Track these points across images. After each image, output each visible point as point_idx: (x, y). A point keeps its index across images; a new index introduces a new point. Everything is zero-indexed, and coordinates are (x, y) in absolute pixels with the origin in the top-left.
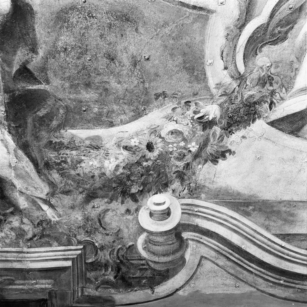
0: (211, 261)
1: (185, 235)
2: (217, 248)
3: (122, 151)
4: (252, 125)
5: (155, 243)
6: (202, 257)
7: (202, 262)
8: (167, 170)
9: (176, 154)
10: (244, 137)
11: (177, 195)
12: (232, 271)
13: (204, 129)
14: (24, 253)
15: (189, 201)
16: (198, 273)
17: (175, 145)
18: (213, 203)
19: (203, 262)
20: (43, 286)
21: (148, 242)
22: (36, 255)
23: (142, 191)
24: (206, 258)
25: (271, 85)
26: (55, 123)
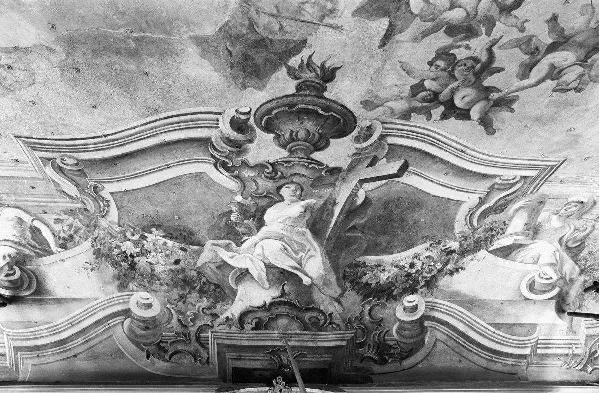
1: (426, 323)
2: (447, 333)
4: (478, 252)
5: (405, 329)
6: (437, 339)
7: (437, 343)
9: (427, 270)
10: (472, 260)
11: (424, 295)
12: (457, 350)
13: (447, 255)
14: (316, 335)
16: (433, 351)
20: (326, 359)
22: (324, 336)
24: (439, 340)
25: (492, 232)
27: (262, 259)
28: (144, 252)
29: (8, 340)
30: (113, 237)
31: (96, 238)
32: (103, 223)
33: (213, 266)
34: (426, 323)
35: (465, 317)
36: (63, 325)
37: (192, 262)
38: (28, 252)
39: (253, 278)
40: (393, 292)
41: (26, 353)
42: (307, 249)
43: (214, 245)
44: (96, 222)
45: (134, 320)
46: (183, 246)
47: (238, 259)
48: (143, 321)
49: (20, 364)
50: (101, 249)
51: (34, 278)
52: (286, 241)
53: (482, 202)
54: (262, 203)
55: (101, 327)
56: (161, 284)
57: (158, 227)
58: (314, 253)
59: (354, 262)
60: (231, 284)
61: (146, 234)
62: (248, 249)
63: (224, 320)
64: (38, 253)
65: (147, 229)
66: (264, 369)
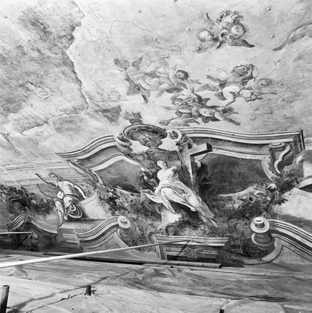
0: (287, 247)
1: (273, 235)
2: (289, 242)
3: (240, 201)
5: (260, 238)
6: (282, 245)
7: (283, 248)
8: (260, 207)
10: (290, 194)
11: (266, 217)
12: (299, 254)
13: (271, 192)
14: (206, 239)
15: (272, 220)
16: (282, 253)
17: (261, 198)
18: (283, 221)
19: (283, 248)
20: (214, 253)
21: (256, 237)
22: (211, 240)
23: (250, 216)
24: (284, 246)
25: (294, 176)
26: (215, 193)
32: (98, 184)
33: (147, 203)
34: (273, 235)
35: (299, 232)
39: (166, 208)
46: (131, 193)
54: (154, 170)
57: (118, 185)
58: (190, 194)
61: (116, 189)
62: (158, 193)
65: (115, 187)
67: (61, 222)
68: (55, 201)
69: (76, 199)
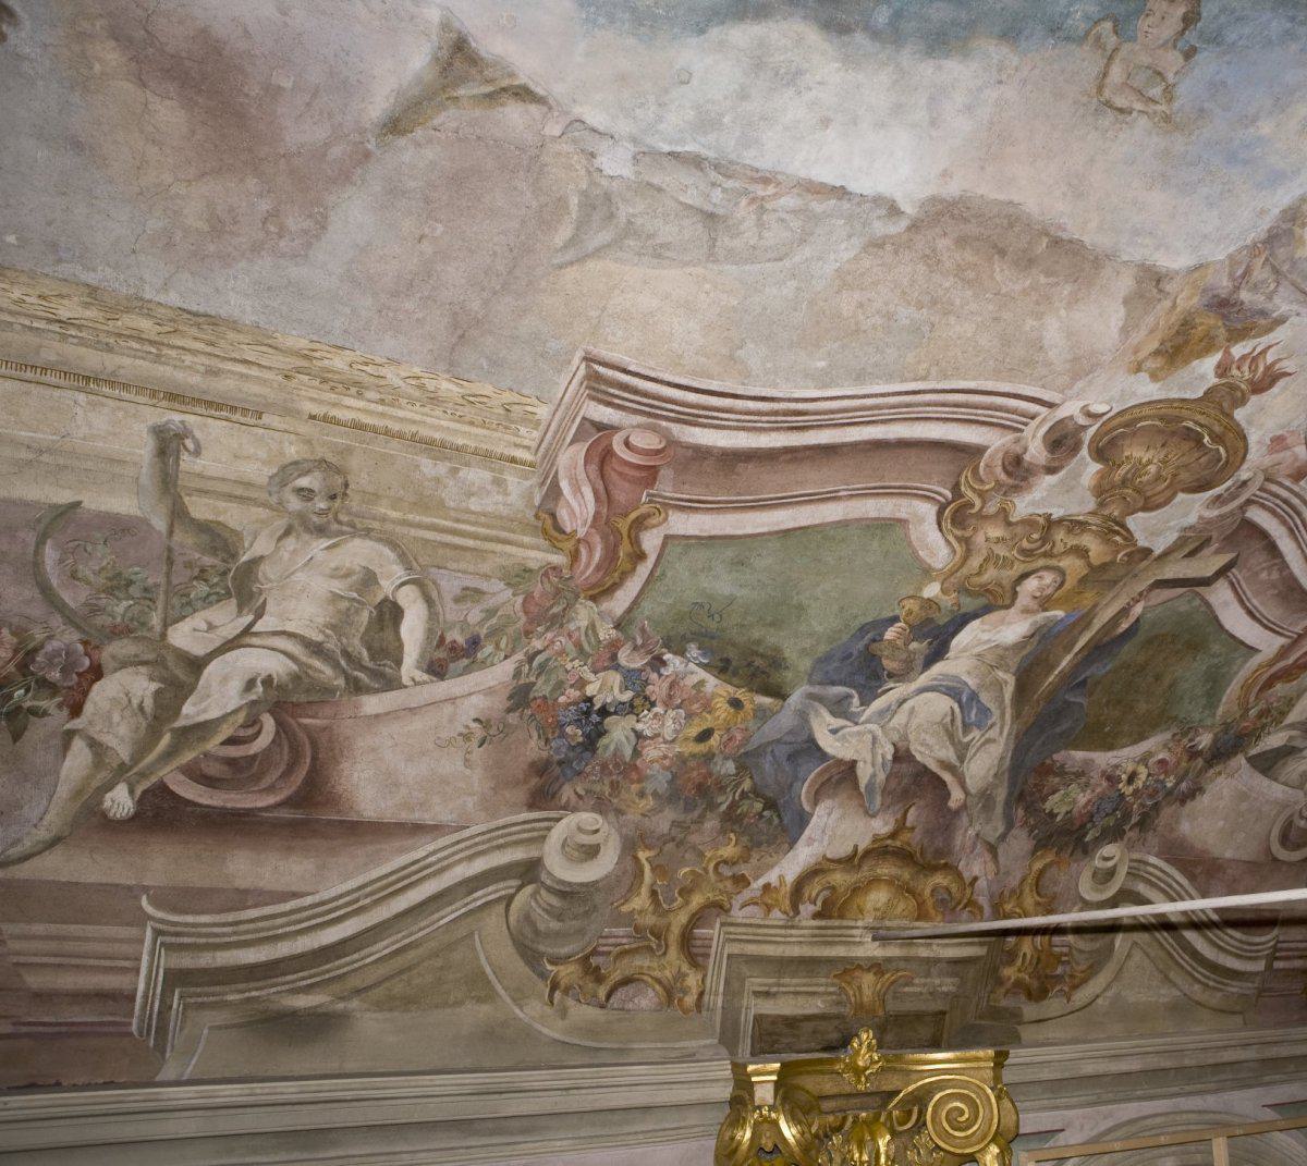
27: (896, 737)
28: (637, 702)
29: (154, 949)
30: (581, 653)
31: (539, 652)
32: (584, 614)
33: (782, 751)
36: (341, 901)
37: (739, 737)
38: (326, 671)
40: (1085, 835)
41: (199, 990)
42: (990, 722)
43: (811, 696)
44: (565, 609)
45: (543, 892)
46: (741, 694)
47: (834, 738)
48: (562, 895)
49: (172, 1024)
50: (534, 684)
51: (308, 754)
52: (964, 700)
53: (1283, 652)
55: (449, 909)
56: (642, 795)
57: (704, 638)
59: (1048, 762)
60: (803, 797)
61: (668, 656)
63: (758, 893)
64: (356, 681)
66: (823, 1017)
67: (43, 834)
68: (111, 664)
69: (326, 671)
